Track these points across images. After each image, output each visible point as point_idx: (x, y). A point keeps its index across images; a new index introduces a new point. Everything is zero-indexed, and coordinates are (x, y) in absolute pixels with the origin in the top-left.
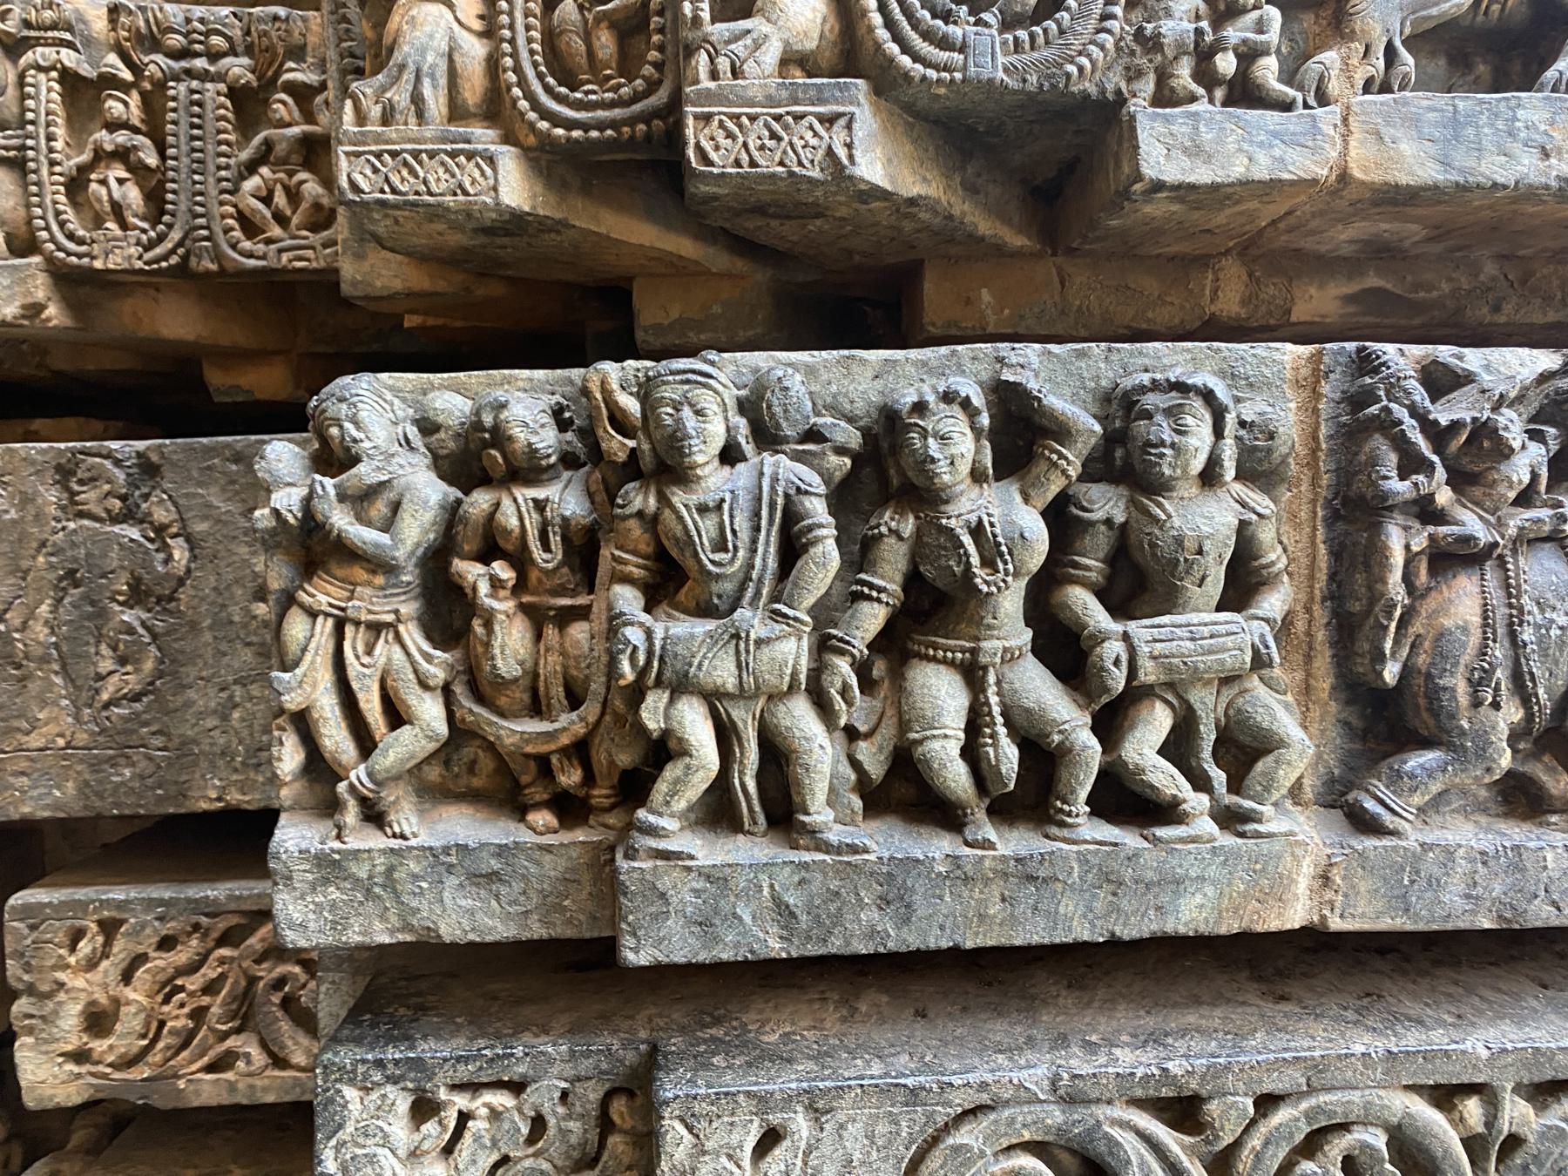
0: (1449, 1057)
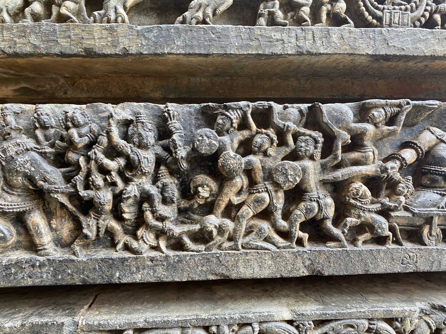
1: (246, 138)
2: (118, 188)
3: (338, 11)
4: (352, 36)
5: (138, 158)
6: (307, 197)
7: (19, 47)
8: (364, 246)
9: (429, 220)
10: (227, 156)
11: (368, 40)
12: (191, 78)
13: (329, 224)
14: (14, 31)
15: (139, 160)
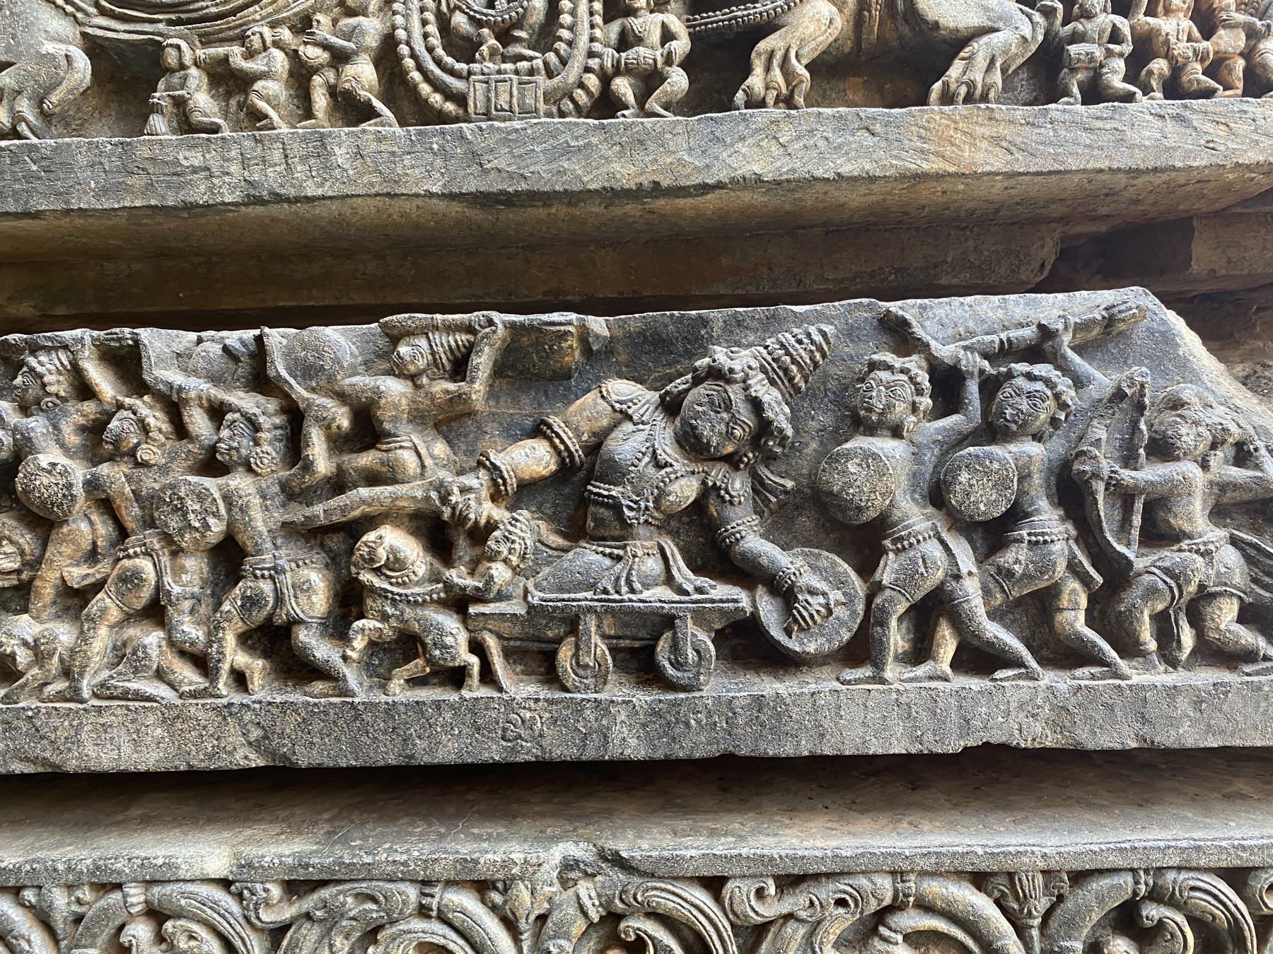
1: (94, 421)
3: (347, 86)
4: (383, 147)
6: (248, 567)
8: (408, 693)
9: (572, 623)
10: (32, 466)
11: (430, 157)
12: (105, 264)
13: (304, 636)
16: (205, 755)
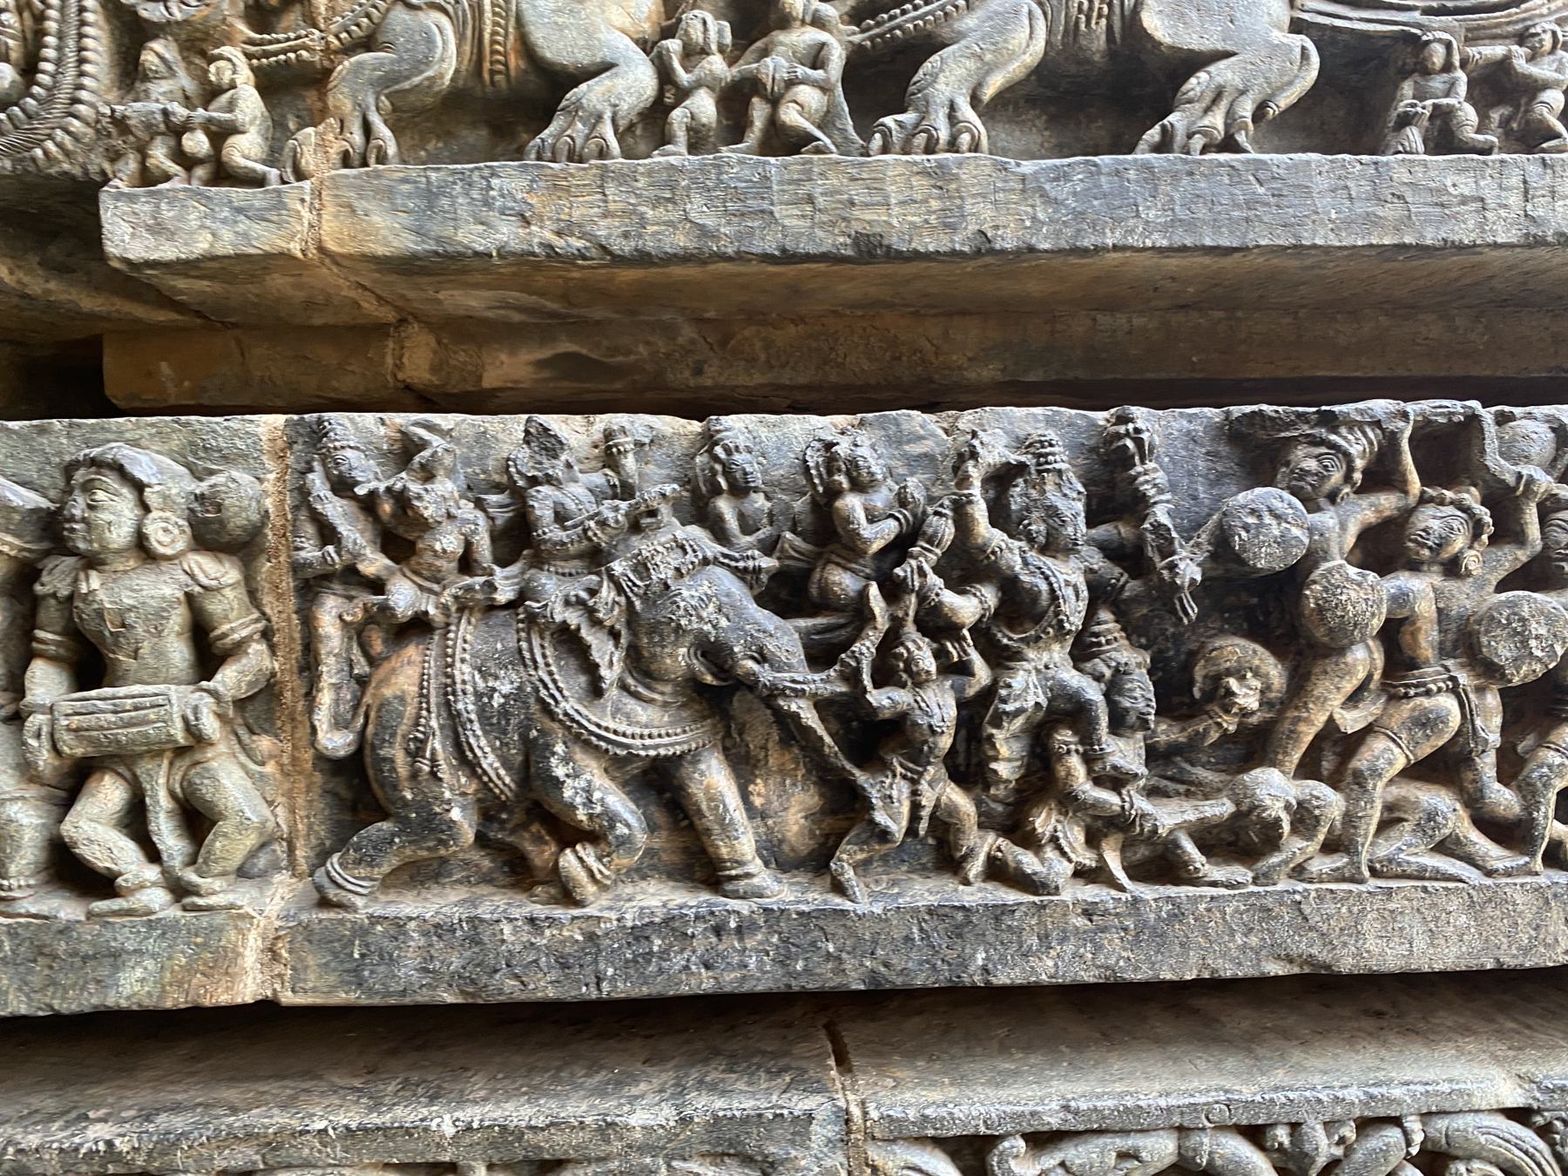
0: (411, 1135)
2: (973, 681)
5: (1050, 584)
7: (654, 234)
12: (1099, 317)
14: (639, 185)
15: (1052, 591)
16: (1518, 949)
